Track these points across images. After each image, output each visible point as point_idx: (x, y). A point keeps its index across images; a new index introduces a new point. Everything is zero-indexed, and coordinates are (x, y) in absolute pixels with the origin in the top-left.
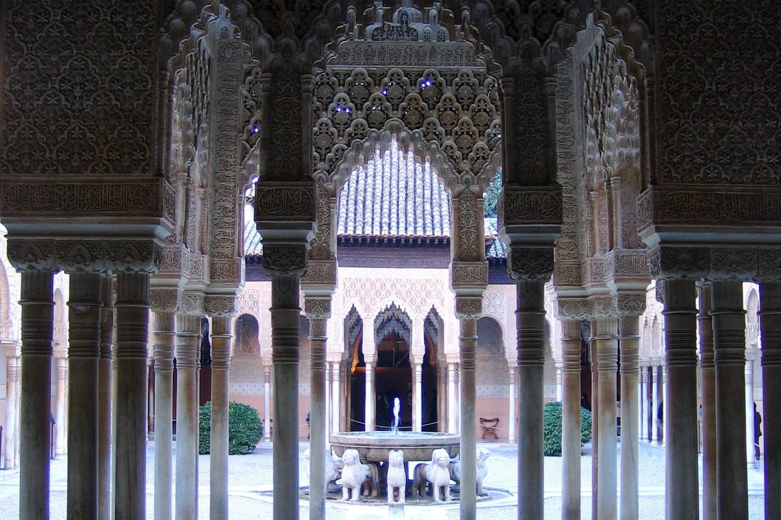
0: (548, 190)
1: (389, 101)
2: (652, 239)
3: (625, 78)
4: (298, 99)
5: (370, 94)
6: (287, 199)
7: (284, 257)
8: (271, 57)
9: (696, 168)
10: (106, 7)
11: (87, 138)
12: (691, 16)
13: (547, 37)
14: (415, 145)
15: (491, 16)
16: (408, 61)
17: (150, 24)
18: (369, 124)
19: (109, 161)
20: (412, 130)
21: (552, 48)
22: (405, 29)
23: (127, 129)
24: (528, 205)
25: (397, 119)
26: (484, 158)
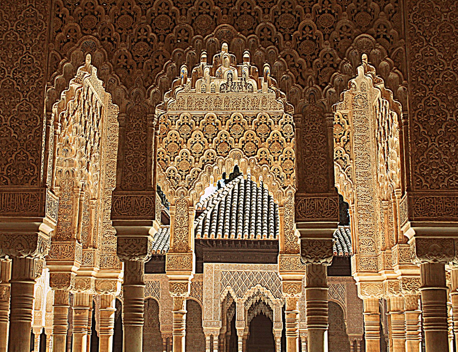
0: (328, 196)
1: (232, 136)
2: (410, 232)
4: (144, 132)
7: (132, 246)
8: (126, 101)
10: (9, 68)
15: (285, 70)
16: (246, 107)
18: (217, 153)
19: (7, 176)
20: (248, 157)
22: (243, 85)
23: (22, 153)
24: (313, 207)
25: (238, 149)
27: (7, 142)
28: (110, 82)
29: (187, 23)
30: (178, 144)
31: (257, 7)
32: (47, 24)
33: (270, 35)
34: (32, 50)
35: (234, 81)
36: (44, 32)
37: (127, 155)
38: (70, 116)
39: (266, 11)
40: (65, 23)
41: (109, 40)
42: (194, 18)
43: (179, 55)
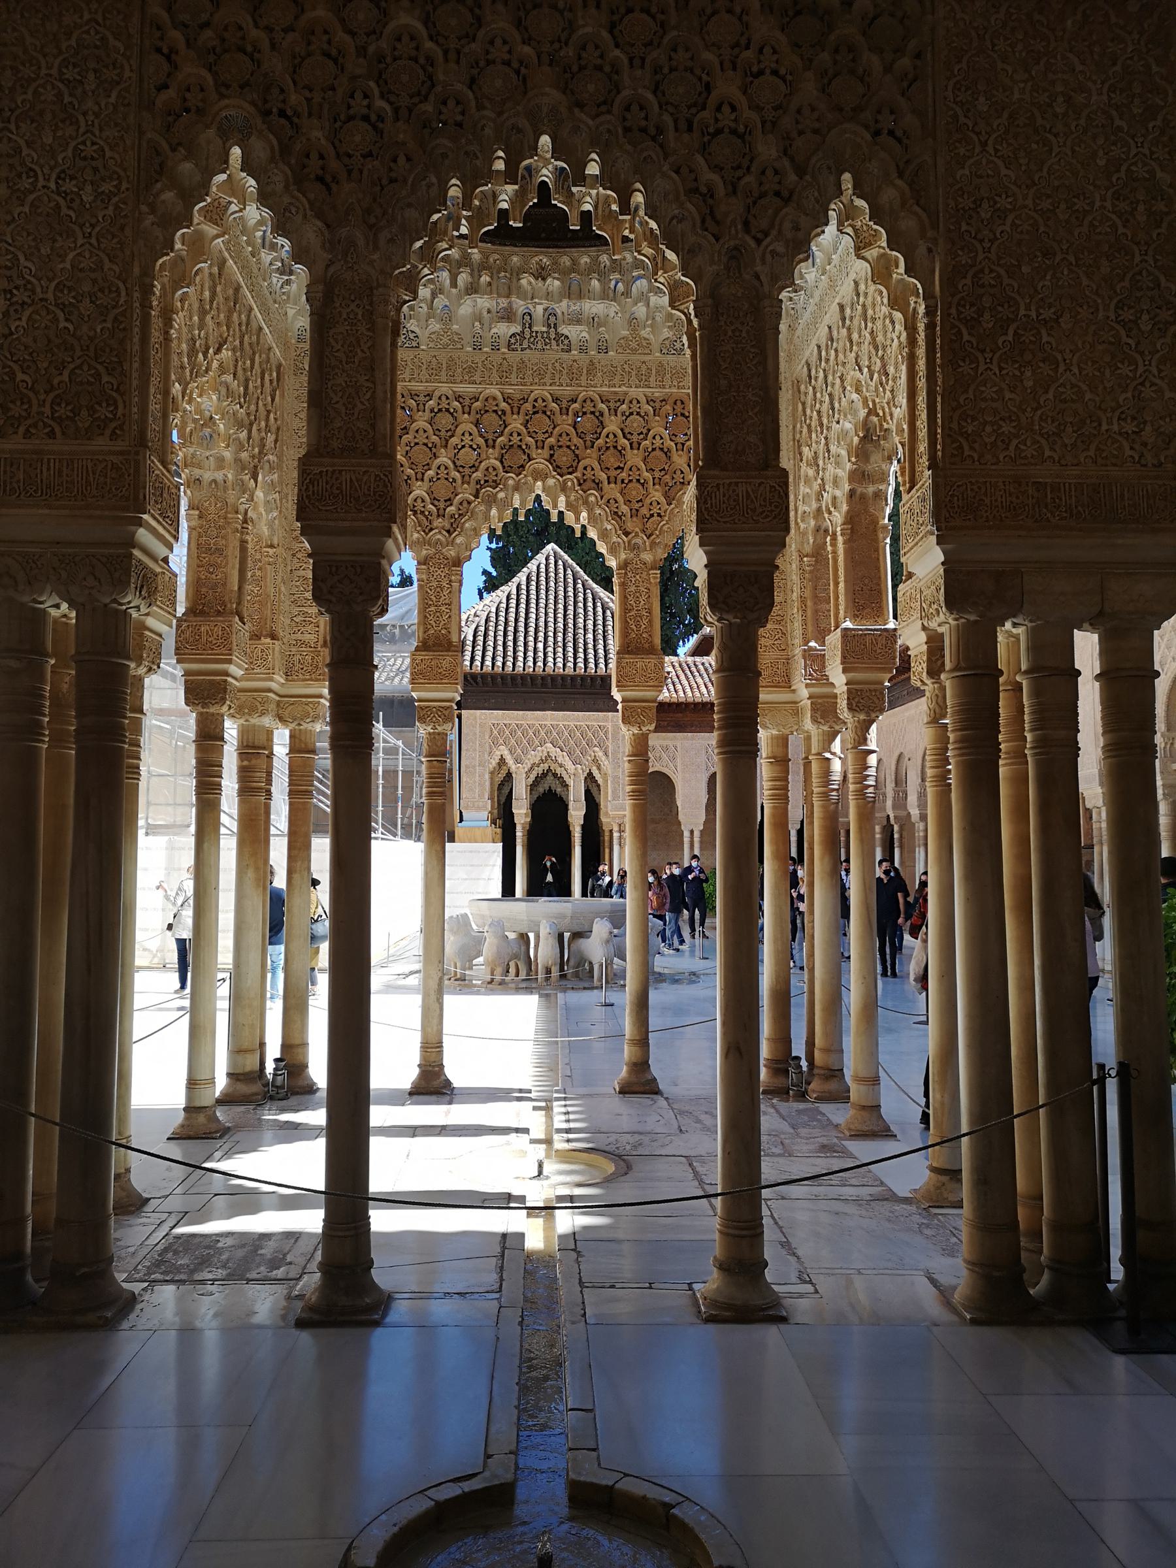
3: (865, 370)
4: (368, 329)
5: (506, 427)
6: (351, 488)
9: (1003, 441)
11: (18, 379)
12: (997, 199)
13: (766, 235)
14: (567, 497)
17: (123, 195)
18: (504, 467)
19: (53, 418)
20: (562, 476)
21: (773, 252)
23: (85, 368)
24: (734, 501)
25: (542, 461)
26: (659, 515)
27: (49, 341)
28: (287, 214)
29: (460, 82)
30: (430, 449)
31: (617, 52)
32: (134, 68)
33: (646, 118)
34: (100, 125)
35: (535, 329)
36: (127, 84)
37: (329, 380)
38: (211, 351)
39: (637, 62)
40: (176, 67)
41: (282, 113)
42: (475, 71)
43: (444, 156)
